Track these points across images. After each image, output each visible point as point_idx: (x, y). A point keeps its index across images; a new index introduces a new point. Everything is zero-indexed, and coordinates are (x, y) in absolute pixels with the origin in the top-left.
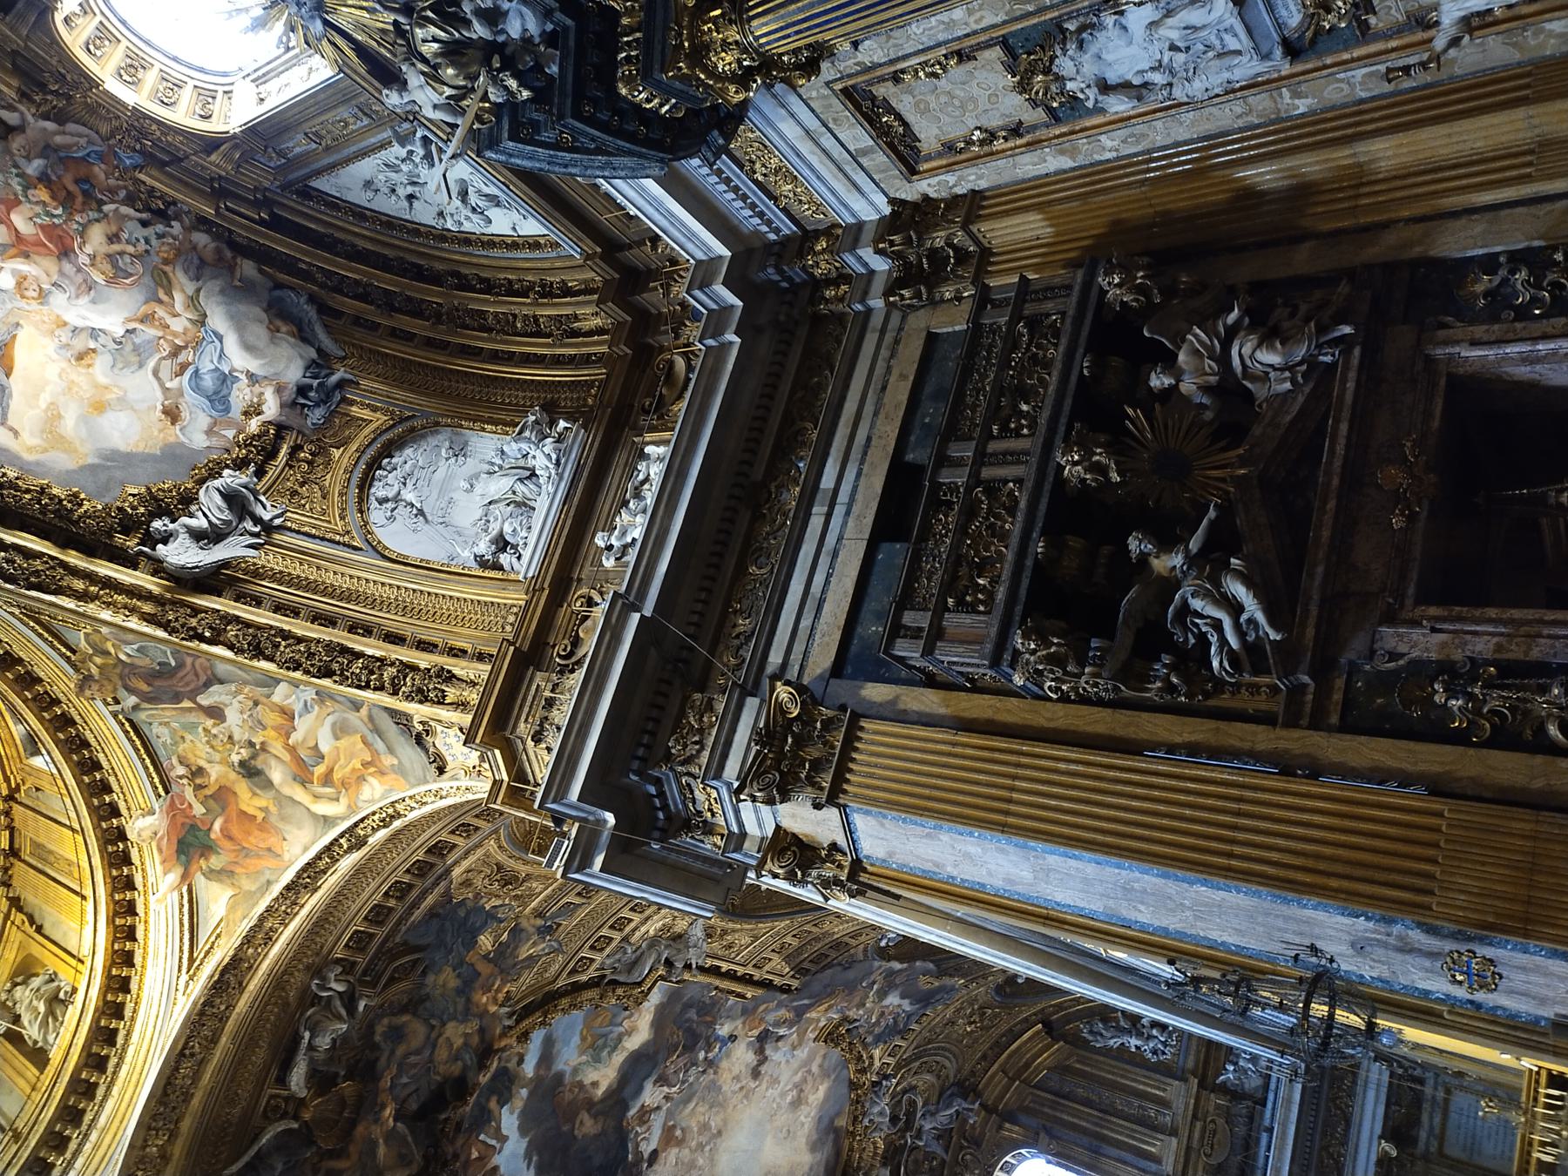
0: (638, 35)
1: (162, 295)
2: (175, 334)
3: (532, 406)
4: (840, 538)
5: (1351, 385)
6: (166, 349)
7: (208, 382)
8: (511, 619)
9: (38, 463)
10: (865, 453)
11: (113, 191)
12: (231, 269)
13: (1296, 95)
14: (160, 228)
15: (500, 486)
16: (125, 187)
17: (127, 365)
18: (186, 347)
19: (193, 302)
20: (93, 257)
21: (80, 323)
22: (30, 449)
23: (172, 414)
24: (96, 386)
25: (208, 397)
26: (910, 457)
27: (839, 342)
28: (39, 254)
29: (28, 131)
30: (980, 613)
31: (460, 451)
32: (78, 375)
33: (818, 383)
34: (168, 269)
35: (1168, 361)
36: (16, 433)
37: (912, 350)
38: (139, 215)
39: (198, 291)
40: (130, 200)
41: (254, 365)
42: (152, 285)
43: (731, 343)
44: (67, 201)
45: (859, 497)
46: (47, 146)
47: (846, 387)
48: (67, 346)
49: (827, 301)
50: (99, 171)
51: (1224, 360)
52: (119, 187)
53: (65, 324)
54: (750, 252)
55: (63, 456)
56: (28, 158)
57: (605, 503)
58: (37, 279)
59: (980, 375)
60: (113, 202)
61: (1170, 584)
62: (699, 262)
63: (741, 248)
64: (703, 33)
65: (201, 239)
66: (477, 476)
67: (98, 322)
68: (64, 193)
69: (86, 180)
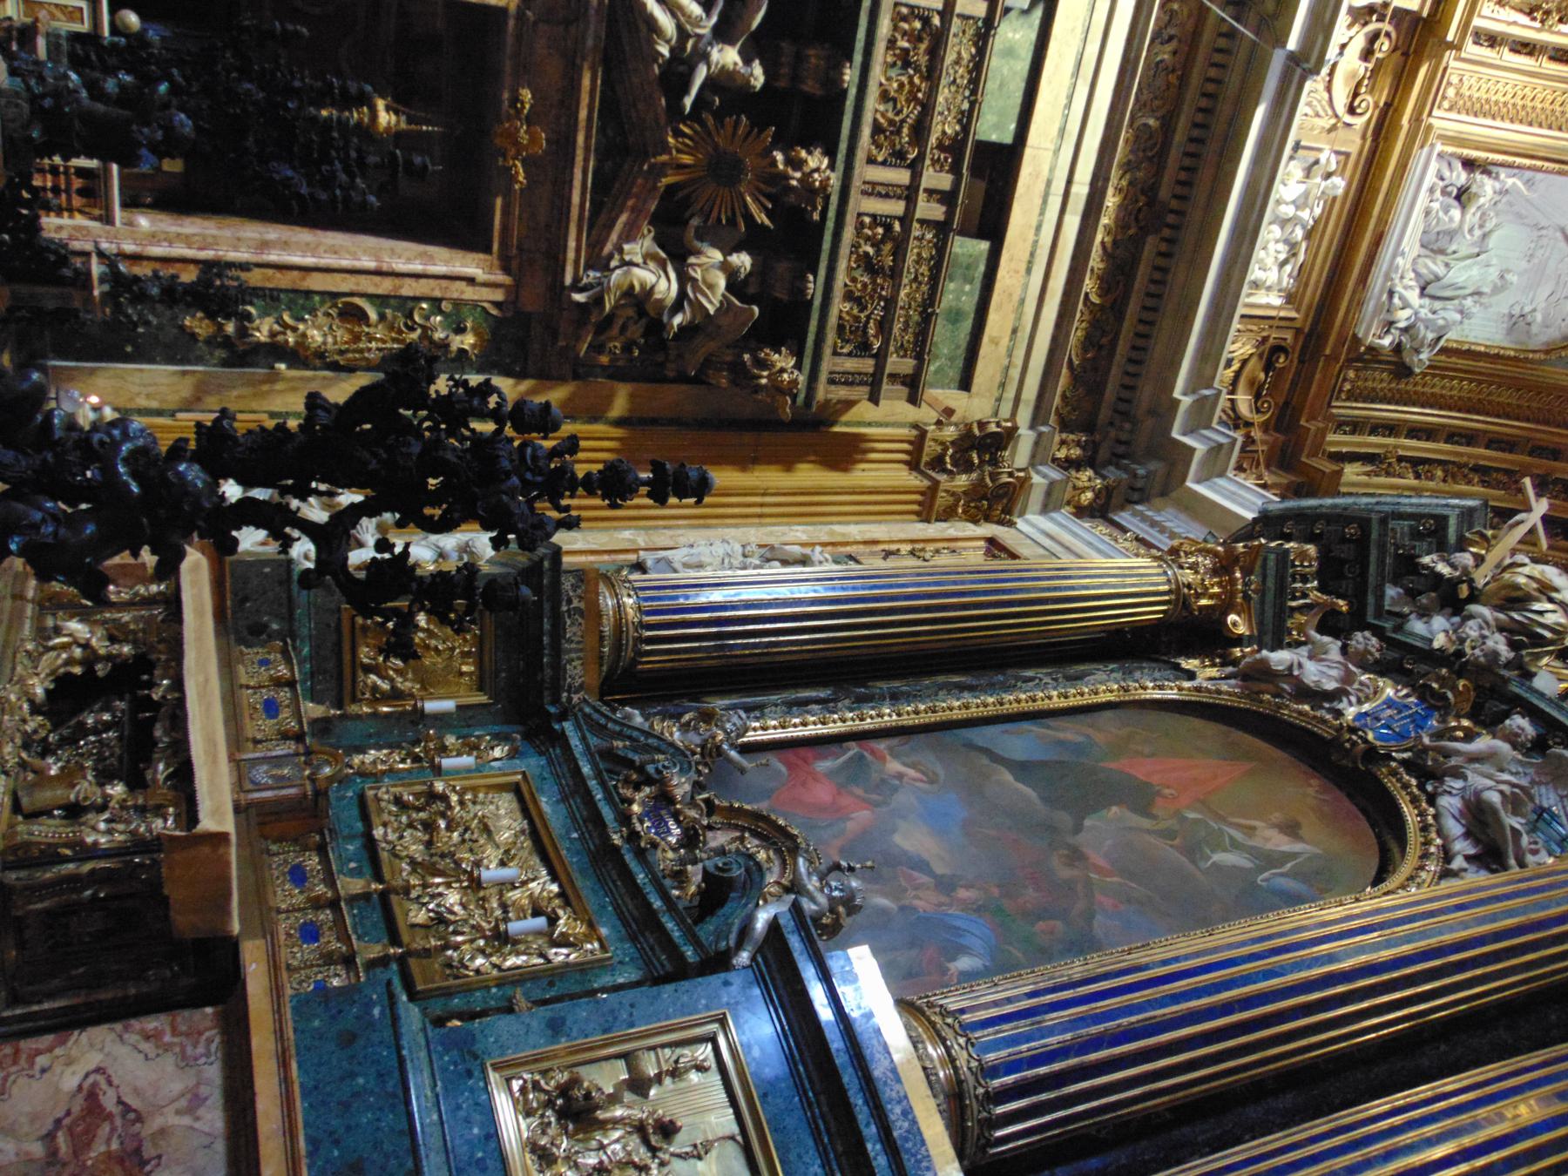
0: (1294, 604)
3: (1424, 375)
4: (1057, 151)
5: (572, 244)
8: (1451, 92)
10: (1032, 254)
13: (633, 541)
15: (1463, 274)
26: (984, 246)
30: (906, 5)
31: (1518, 322)
35: (735, 285)
37: (985, 371)
43: (1185, 394)
45: (1038, 201)
49: (1078, 444)
51: (684, 278)
54: (1164, 493)
57: (1332, 230)
59: (914, 299)
61: (723, 34)
62: (1222, 474)
63: (1174, 495)
64: (1220, 584)
66: (1497, 290)
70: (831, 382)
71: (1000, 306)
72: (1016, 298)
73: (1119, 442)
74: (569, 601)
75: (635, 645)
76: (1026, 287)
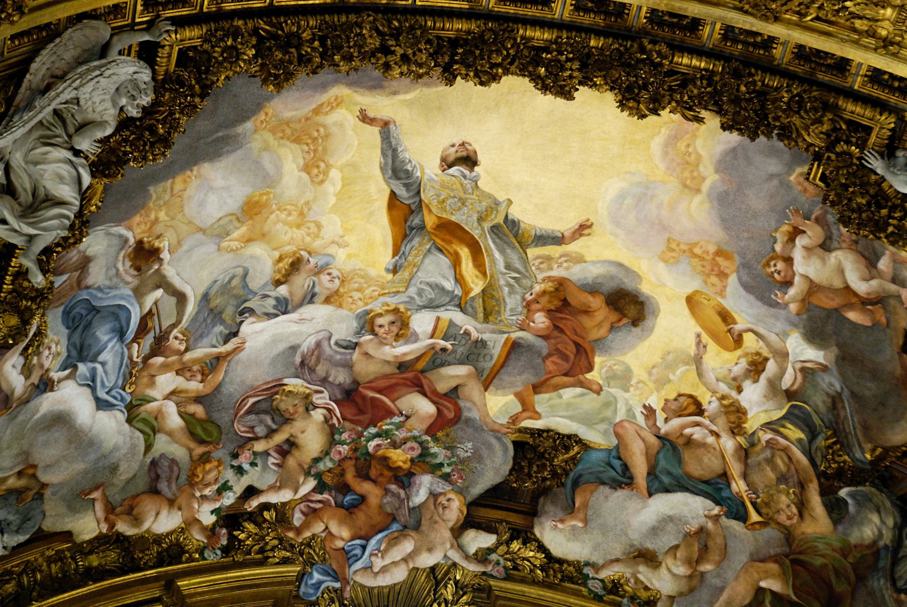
1: (198, 410)
2: (165, 368)
6: (175, 343)
7: (103, 333)
9: (324, 87)
11: (312, 514)
12: (110, 509)
14: (229, 499)
16: (298, 531)
17: (226, 289)
18: (146, 359)
19: (151, 428)
20: (309, 406)
21: (307, 311)
22: (339, 102)
23: (145, 255)
24: (263, 236)
25: (95, 310)
28: (386, 376)
29: (448, 534)
32: (289, 237)
34: (200, 450)
36: (365, 118)
38: (263, 499)
39: (148, 447)
40: (282, 512)
41: (47, 403)
42: (215, 416)
44: (366, 464)
46: (417, 527)
48: (319, 271)
50: (342, 532)
52: (306, 525)
53: (327, 301)
55: (288, 114)
56: (434, 496)
58: (382, 343)
60: (306, 499)
65: (164, 522)
67: (287, 328)
68: (373, 473)
69: (350, 509)
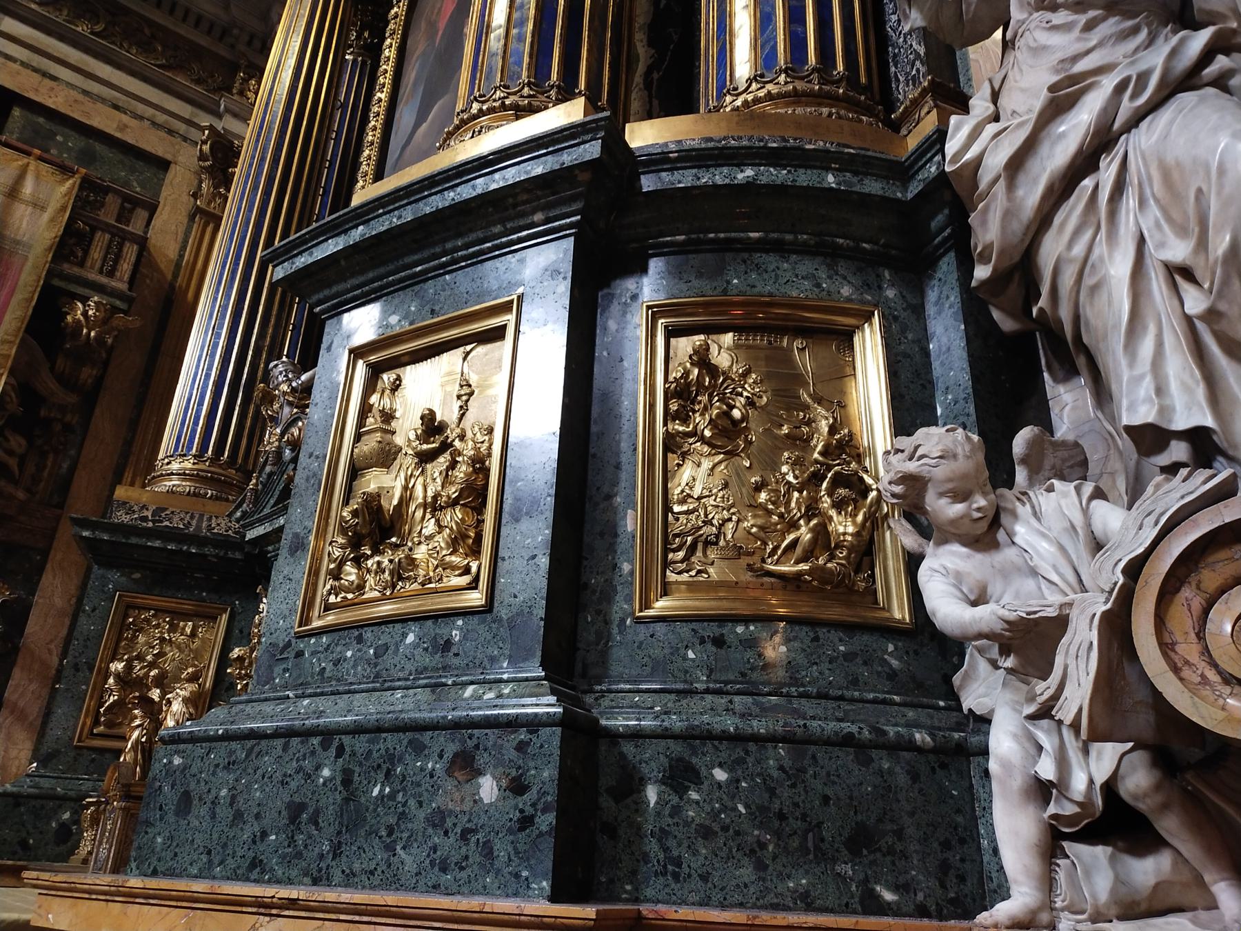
10: (35, 70)
26: (16, 112)
27: (198, 82)
33: (155, 50)
37: (154, 143)
47: (133, 73)
70: (111, 274)
71: (88, 114)
72: (80, 97)
73: (249, 43)
74: (145, 519)
75: (220, 466)
76: (69, 85)
